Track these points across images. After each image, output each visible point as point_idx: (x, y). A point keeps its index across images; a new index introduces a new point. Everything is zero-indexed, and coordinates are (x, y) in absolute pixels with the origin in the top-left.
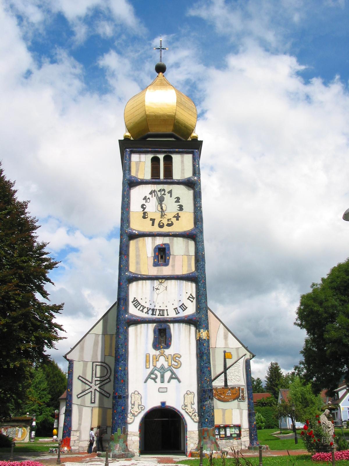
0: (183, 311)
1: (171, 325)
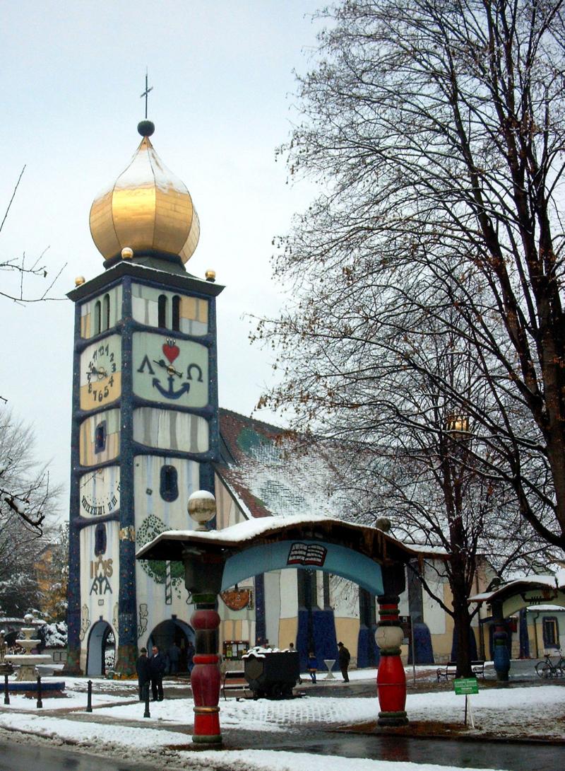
1: (106, 524)
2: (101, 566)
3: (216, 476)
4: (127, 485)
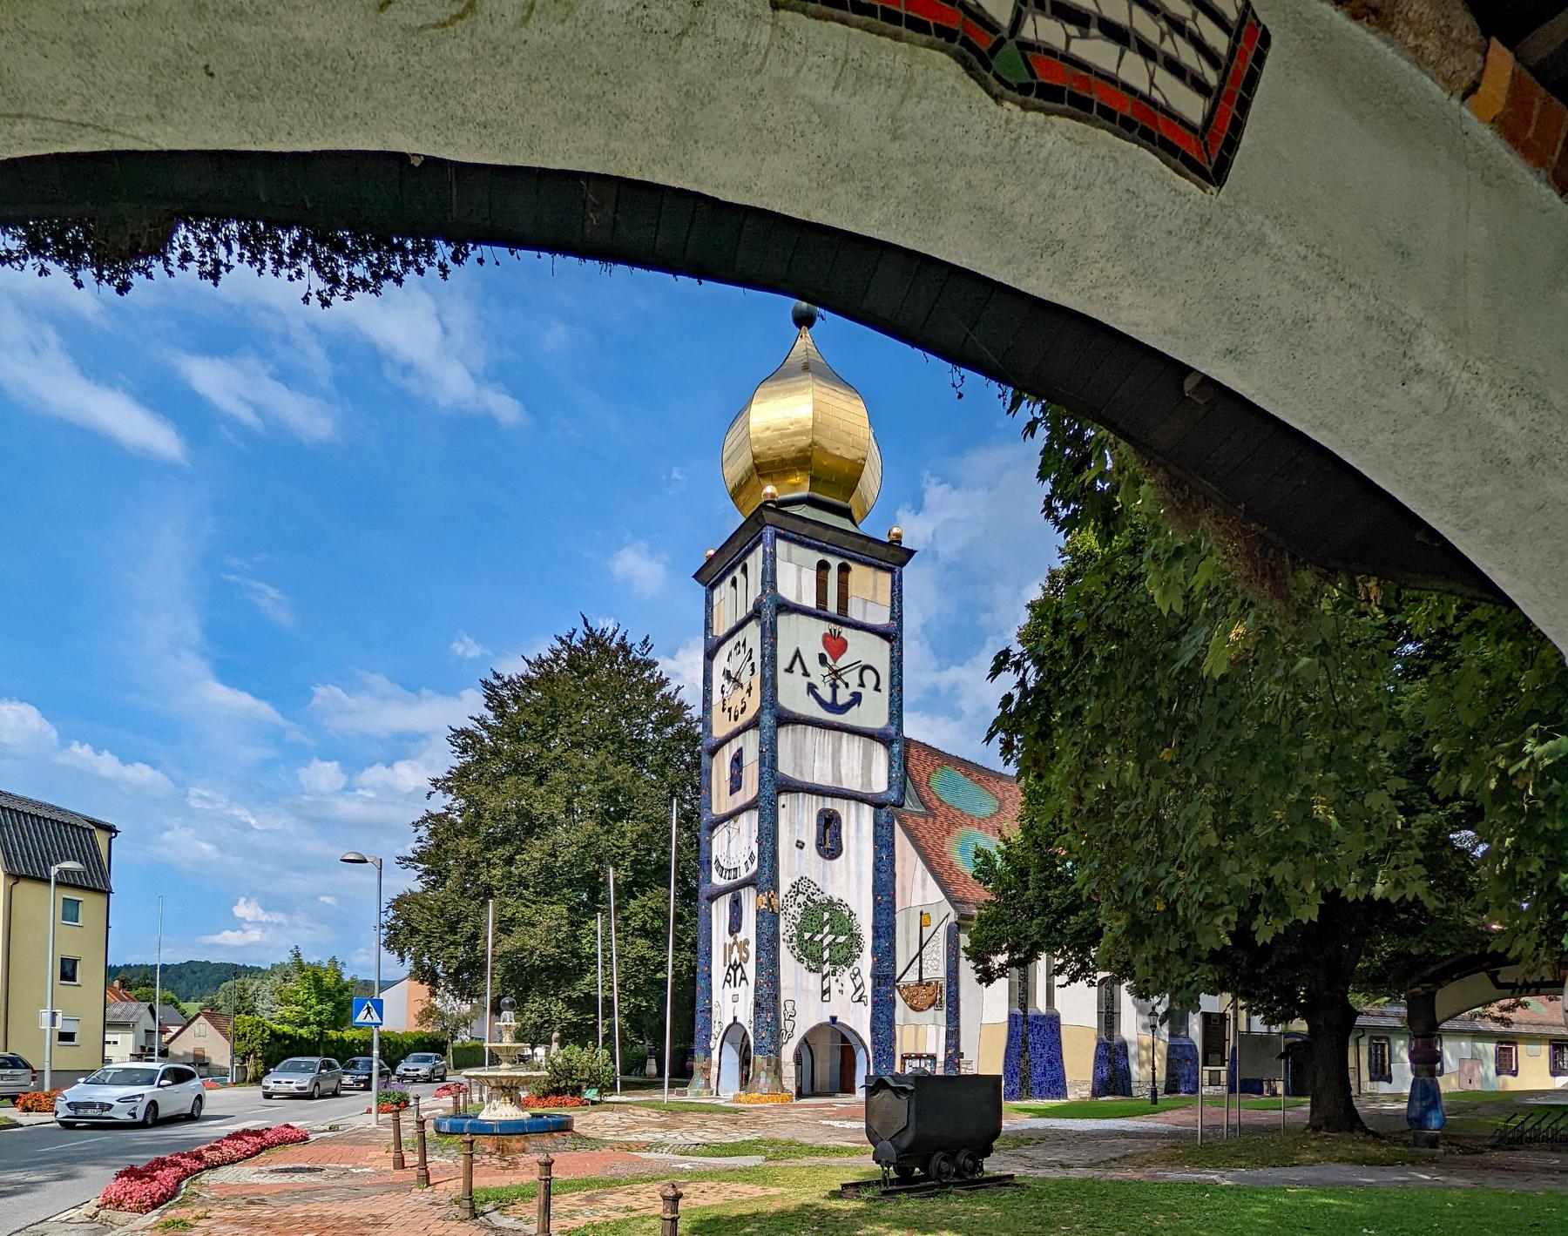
1: (742, 891)
2: (735, 947)
3: (897, 825)
4: (768, 837)
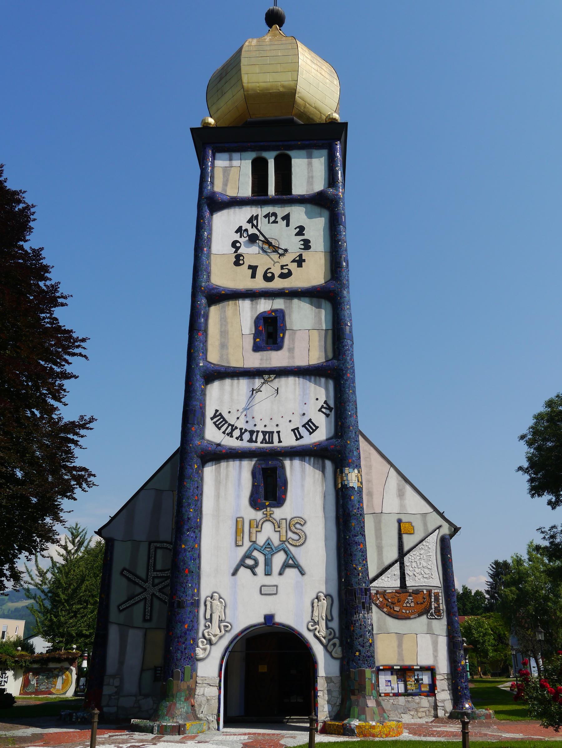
0: (311, 433)
